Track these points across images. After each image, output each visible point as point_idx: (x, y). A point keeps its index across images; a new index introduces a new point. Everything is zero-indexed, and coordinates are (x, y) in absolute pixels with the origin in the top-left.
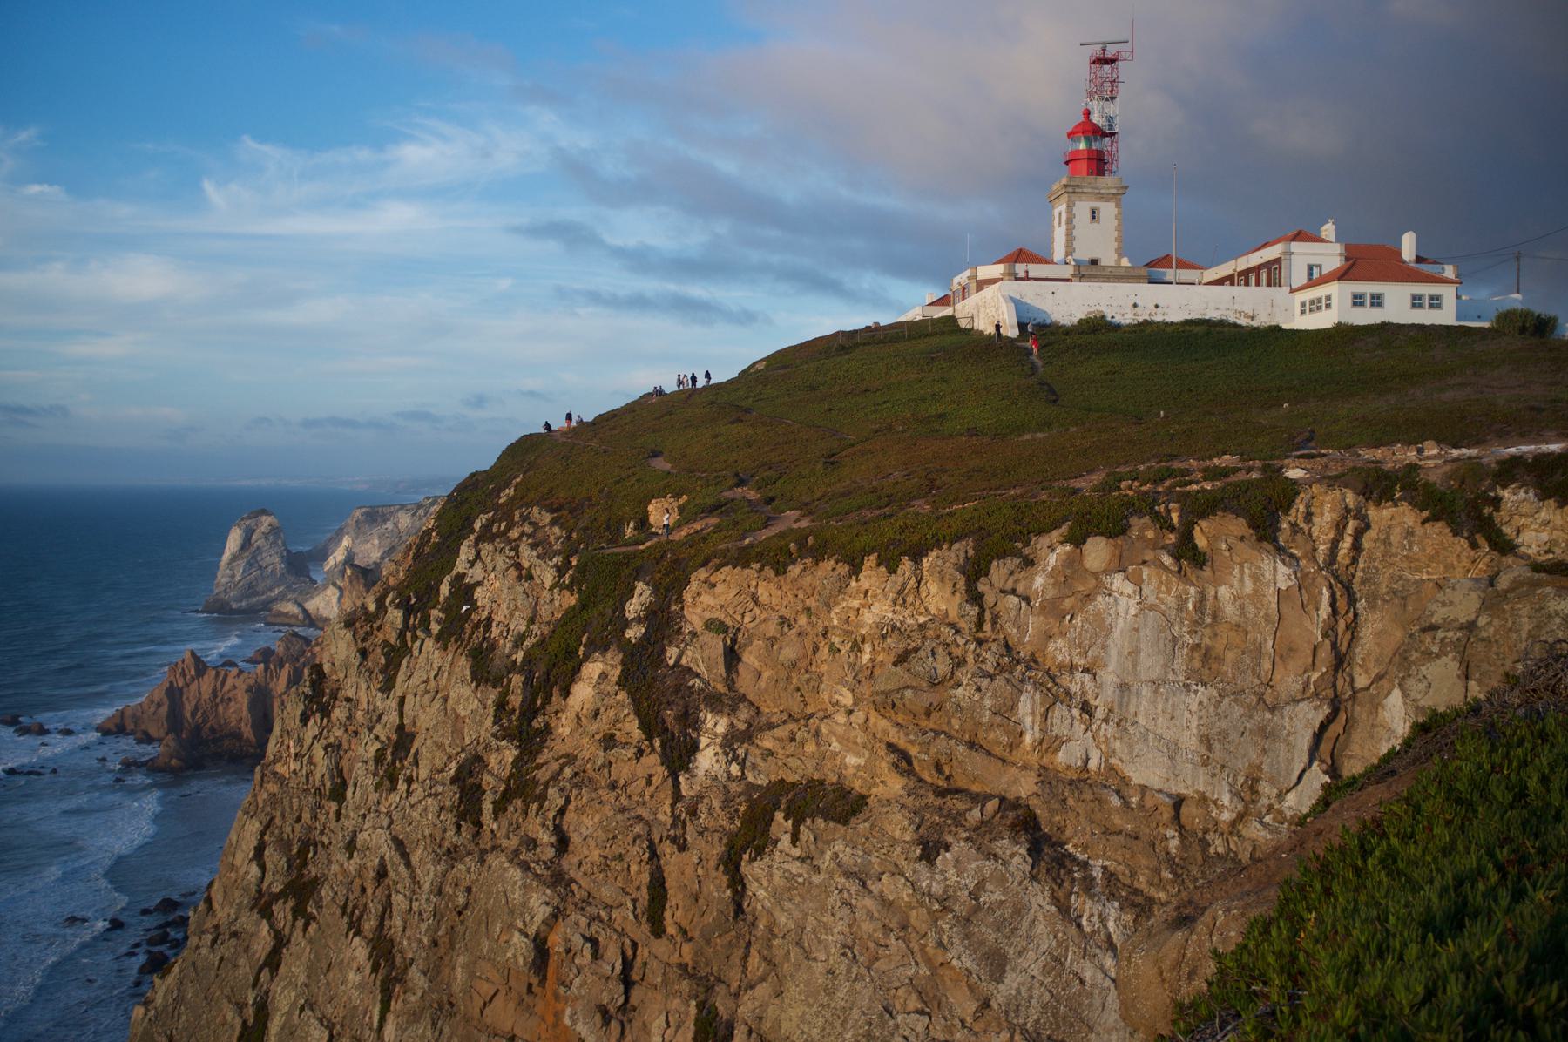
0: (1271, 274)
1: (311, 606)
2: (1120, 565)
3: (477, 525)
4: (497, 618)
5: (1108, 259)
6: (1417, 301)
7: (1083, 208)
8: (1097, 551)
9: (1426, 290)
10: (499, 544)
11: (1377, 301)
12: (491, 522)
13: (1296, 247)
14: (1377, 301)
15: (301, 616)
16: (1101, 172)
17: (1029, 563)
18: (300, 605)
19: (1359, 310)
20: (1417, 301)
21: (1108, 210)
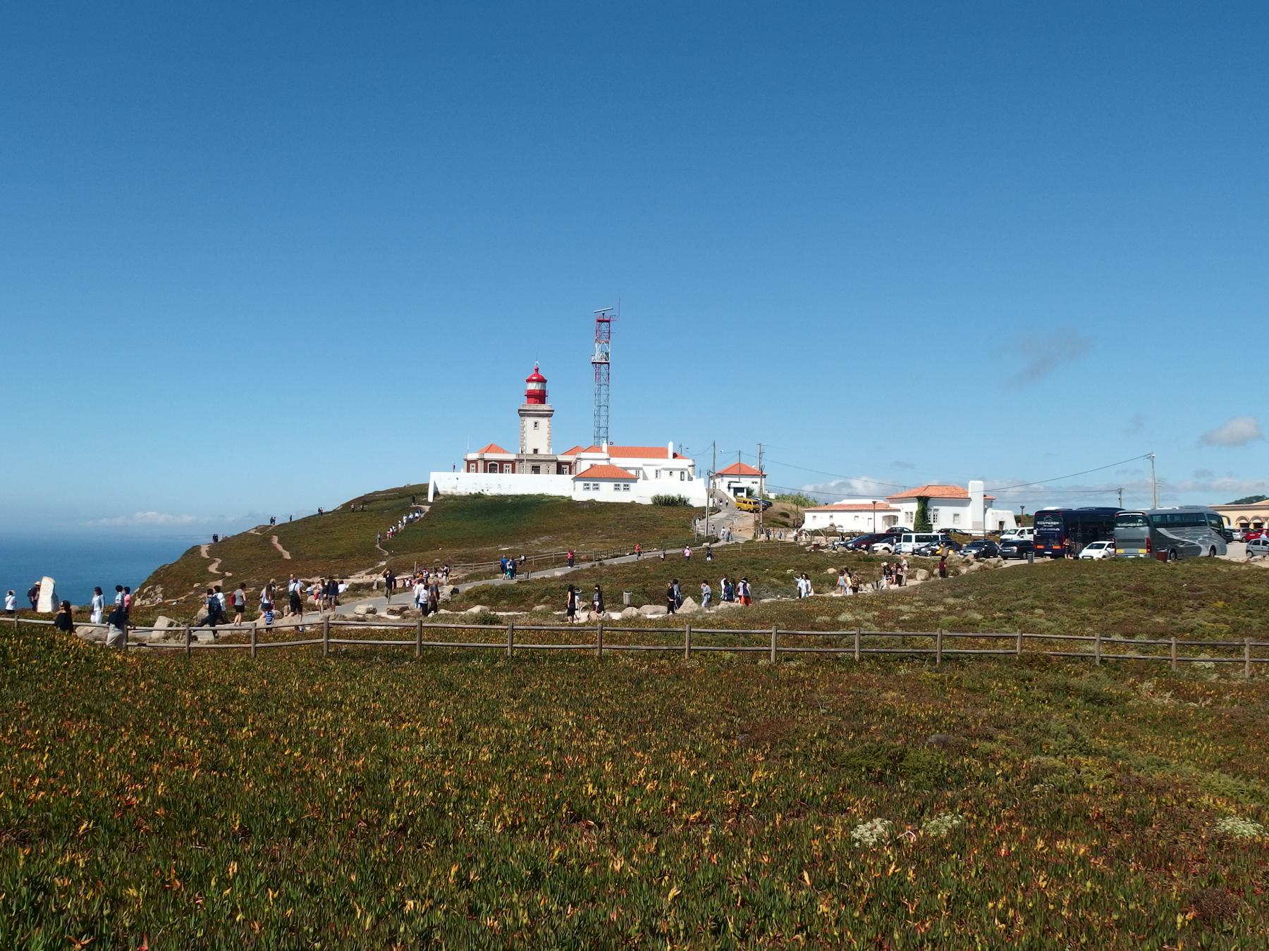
6: (617, 488)
7: (530, 421)
16: (543, 402)
19: (587, 492)
20: (617, 488)
21: (543, 422)
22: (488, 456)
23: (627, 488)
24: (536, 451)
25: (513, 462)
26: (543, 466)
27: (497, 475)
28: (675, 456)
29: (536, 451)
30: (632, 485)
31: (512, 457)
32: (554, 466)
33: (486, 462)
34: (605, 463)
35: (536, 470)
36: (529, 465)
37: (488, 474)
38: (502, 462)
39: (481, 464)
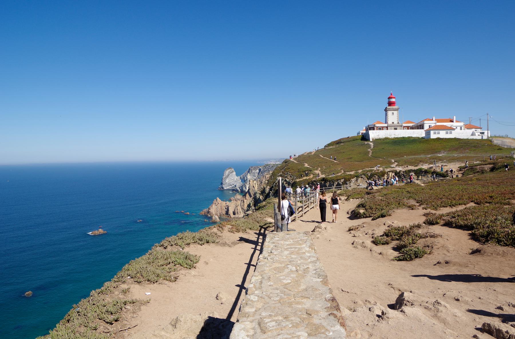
5: (396, 123)
6: (447, 133)
9: (449, 131)
13: (425, 122)
16: (394, 105)
19: (435, 135)
20: (447, 133)
21: (395, 112)
22: (377, 125)
23: (451, 133)
25: (387, 127)
26: (398, 128)
28: (457, 121)
30: (453, 131)
31: (386, 125)
33: (377, 127)
34: (434, 125)
35: (396, 129)
36: (393, 128)
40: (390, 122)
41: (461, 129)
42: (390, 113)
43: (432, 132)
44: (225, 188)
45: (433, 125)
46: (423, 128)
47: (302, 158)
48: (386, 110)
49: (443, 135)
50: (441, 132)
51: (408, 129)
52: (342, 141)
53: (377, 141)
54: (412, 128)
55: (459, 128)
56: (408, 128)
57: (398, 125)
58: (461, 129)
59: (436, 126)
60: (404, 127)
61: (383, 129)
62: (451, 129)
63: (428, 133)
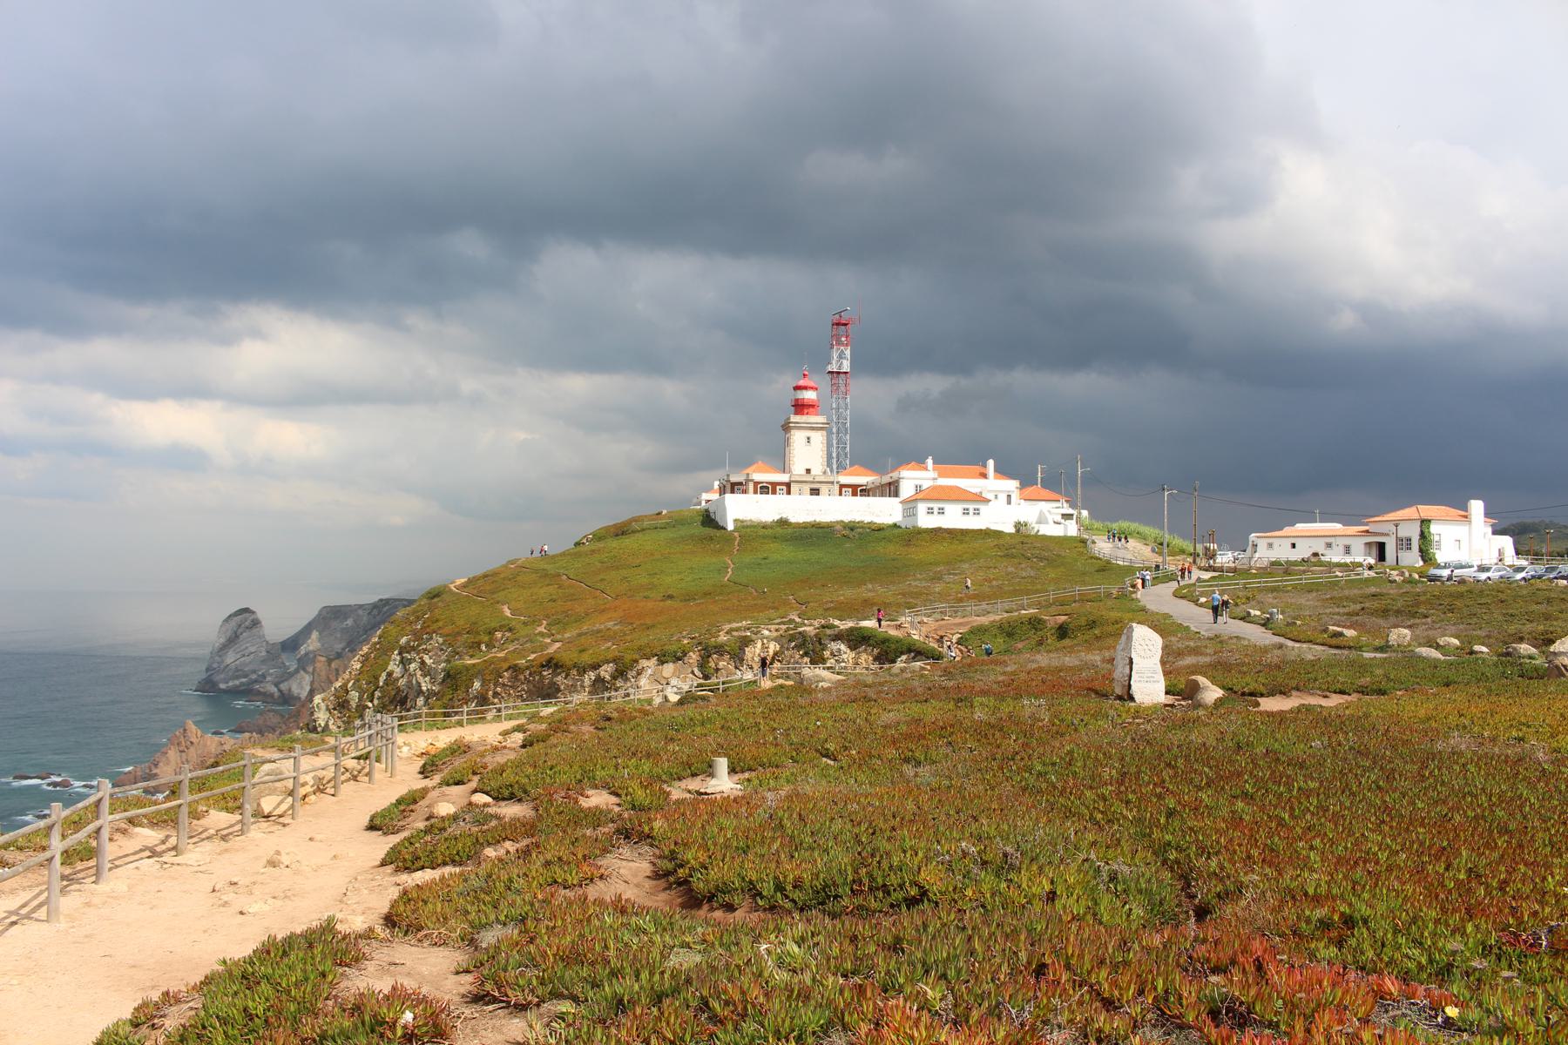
0: (892, 489)
1: (284, 686)
2: (676, 674)
3: (403, 640)
4: (411, 697)
5: (818, 469)
6: (966, 512)
8: (669, 668)
9: (971, 507)
10: (414, 654)
11: (941, 512)
12: (408, 642)
14: (941, 512)
15: (277, 694)
17: (639, 674)
18: (276, 685)
20: (966, 512)
22: (757, 477)
23: (977, 512)
24: (808, 471)
25: (788, 485)
26: (824, 489)
27: (769, 498)
29: (808, 471)
30: (983, 508)
31: (784, 478)
32: (837, 487)
33: (756, 484)
35: (815, 492)
36: (807, 488)
37: (759, 496)
38: (774, 485)
39: (751, 486)
40: (798, 469)
41: (1009, 502)
42: (798, 437)
43: (922, 508)
44: (222, 686)
45: (926, 485)
46: (896, 495)
47: (488, 585)
48: (786, 427)
49: (953, 518)
50: (949, 507)
51: (855, 494)
52: (635, 526)
53: (752, 533)
54: (865, 491)
55: (1003, 497)
56: (856, 490)
57: (823, 479)
58: (1009, 502)
59: (934, 488)
60: (842, 486)
61: (774, 492)
62: (980, 499)
63: (910, 506)
